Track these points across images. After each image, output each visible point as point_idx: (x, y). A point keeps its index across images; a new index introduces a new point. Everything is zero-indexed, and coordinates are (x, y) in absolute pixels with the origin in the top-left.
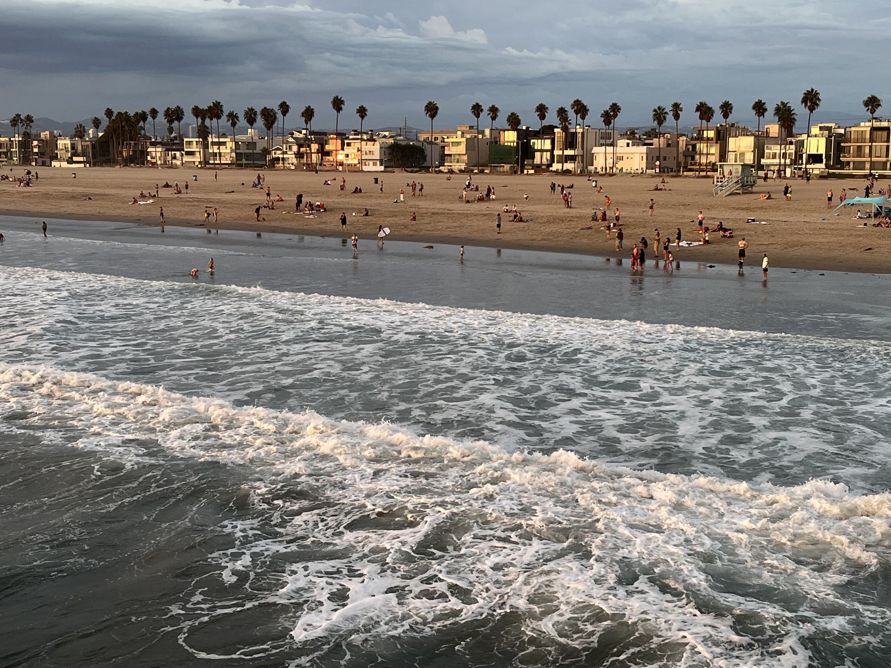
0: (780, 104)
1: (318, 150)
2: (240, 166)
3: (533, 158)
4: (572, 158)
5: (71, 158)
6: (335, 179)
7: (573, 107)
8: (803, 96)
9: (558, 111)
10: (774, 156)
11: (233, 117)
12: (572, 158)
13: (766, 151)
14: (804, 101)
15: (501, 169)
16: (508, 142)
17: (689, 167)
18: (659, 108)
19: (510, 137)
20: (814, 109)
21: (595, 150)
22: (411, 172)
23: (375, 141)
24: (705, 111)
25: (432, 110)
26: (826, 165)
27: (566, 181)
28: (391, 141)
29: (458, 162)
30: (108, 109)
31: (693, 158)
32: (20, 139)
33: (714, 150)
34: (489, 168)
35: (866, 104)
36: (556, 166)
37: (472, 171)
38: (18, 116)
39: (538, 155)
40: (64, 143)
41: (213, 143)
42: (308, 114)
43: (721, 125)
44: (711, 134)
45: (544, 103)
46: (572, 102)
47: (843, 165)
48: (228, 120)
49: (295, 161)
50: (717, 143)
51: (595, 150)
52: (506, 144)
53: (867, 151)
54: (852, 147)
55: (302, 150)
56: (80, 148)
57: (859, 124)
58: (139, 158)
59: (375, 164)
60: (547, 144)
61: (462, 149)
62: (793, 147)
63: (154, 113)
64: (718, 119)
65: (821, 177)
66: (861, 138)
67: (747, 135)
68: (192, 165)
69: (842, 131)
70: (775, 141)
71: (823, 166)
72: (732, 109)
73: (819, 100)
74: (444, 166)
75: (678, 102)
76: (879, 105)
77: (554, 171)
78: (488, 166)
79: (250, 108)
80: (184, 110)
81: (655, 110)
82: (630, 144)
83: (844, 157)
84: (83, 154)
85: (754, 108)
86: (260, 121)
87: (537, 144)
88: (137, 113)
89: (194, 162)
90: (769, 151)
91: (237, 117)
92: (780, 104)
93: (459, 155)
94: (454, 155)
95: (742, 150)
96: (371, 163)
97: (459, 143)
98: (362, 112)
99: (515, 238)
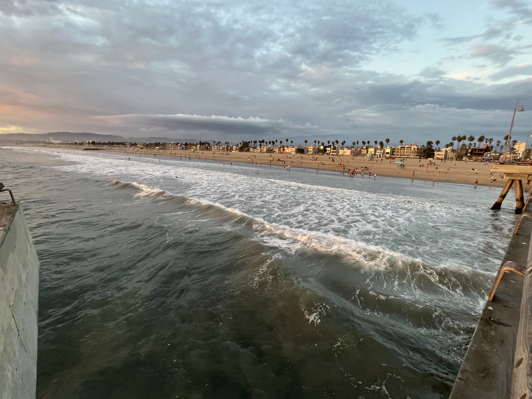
2: (267, 152)
4: (335, 152)
10: (378, 153)
14: (386, 141)
19: (322, 147)
21: (340, 150)
24: (364, 143)
25: (306, 142)
27: (333, 157)
36: (331, 154)
39: (327, 151)
40: (234, 147)
42: (281, 142)
44: (365, 148)
47: (394, 155)
51: (340, 150)
53: (399, 152)
58: (248, 150)
60: (330, 149)
63: (251, 142)
64: (367, 145)
66: (398, 149)
69: (394, 147)
71: (389, 155)
84: (238, 150)
86: (272, 143)
87: (327, 149)
98: (292, 142)
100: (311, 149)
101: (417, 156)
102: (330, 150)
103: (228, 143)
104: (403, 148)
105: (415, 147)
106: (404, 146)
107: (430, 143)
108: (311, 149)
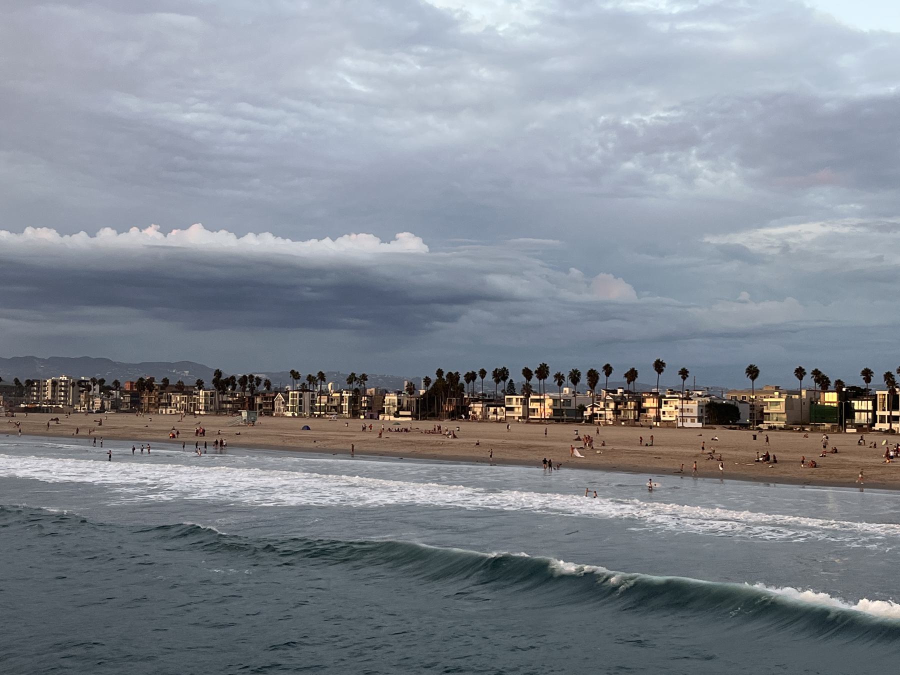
1: (635, 407)
2: (558, 421)
3: (854, 417)
5: (397, 412)
6: (701, 435)
11: (559, 378)
19: (831, 398)
22: (731, 428)
23: (690, 399)
25: (753, 372)
28: (708, 399)
29: (777, 420)
30: (439, 369)
32: (351, 395)
34: (810, 427)
36: (878, 426)
38: (353, 374)
39: (856, 414)
42: (632, 375)
48: (555, 381)
49: (612, 417)
52: (826, 404)
55: (619, 407)
56: (405, 403)
59: (693, 421)
60: (869, 405)
61: (781, 408)
63: (483, 373)
68: (512, 419)
77: (877, 431)
78: (809, 424)
80: (509, 371)
87: (857, 405)
88: (468, 373)
89: (514, 417)
91: (563, 377)
94: (772, 413)
96: (689, 420)
97: (778, 403)
98: (684, 373)
102: (874, 411)
103: (364, 377)
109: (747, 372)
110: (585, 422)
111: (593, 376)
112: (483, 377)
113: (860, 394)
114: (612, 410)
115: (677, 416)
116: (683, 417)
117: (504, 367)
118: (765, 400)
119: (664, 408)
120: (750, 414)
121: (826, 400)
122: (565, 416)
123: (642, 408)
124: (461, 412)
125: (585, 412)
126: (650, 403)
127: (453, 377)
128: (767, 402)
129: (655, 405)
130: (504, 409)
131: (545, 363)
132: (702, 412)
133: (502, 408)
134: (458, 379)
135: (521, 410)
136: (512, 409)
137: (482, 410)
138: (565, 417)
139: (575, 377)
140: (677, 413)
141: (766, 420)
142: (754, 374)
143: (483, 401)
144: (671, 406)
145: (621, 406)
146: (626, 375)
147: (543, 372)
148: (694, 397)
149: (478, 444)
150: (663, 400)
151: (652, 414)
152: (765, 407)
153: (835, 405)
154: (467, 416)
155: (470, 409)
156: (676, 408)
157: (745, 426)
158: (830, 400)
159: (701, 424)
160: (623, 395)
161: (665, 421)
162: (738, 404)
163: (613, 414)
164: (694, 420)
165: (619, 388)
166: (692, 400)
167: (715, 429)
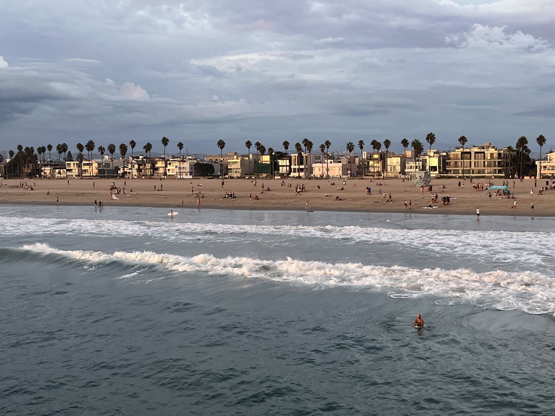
0: (414, 140)
2: (102, 177)
3: (279, 170)
4: (302, 170)
6: (191, 183)
7: (303, 142)
8: (426, 136)
9: (296, 145)
10: (411, 168)
11: (101, 149)
12: (302, 170)
13: (407, 165)
14: (427, 139)
15: (261, 176)
16: (265, 161)
17: (366, 174)
18: (350, 143)
19: (266, 159)
20: (432, 143)
21: (314, 165)
22: (209, 178)
23: (185, 161)
24: (376, 145)
25: (221, 144)
26: (439, 171)
27: (300, 182)
29: (236, 172)
31: (368, 169)
33: (380, 165)
34: (255, 176)
35: (460, 140)
36: (292, 174)
37: (244, 178)
39: (281, 168)
41: (85, 164)
42: (148, 147)
43: (382, 152)
45: (287, 141)
46: (303, 140)
47: (447, 172)
48: (99, 151)
49: (136, 173)
50: (380, 161)
51: (314, 165)
52: (263, 162)
53: (460, 164)
54: (452, 163)
55: (141, 167)
57: (455, 150)
59: (186, 175)
60: (286, 162)
61: (238, 165)
62: (421, 163)
63: (50, 147)
64: (383, 149)
65: (437, 178)
67: (395, 157)
69: (445, 154)
70: (410, 159)
71: (437, 172)
72: (390, 143)
73: (435, 138)
74: (228, 175)
75: (362, 140)
76: (466, 141)
77: (292, 177)
79: (111, 144)
80: (68, 145)
81: (348, 144)
82: (332, 162)
83: (448, 167)
85: (402, 142)
89: (72, 175)
90: (408, 165)
91: (104, 149)
92: (414, 140)
93: (236, 168)
95: (394, 164)
96: (184, 174)
97: (236, 162)
98: (180, 146)
99: (345, 207)
100: (235, 164)
101: (500, 171)
104: (466, 155)
105: (492, 150)
106: (468, 150)
107: (523, 141)
108: (235, 164)
109: (218, 144)
110: (119, 177)
111: (123, 148)
112: (50, 150)
113: (282, 156)
114: (136, 169)
115: (177, 172)
116: (180, 172)
117: (64, 143)
118: (229, 161)
119: (169, 167)
120: (220, 170)
121: (264, 160)
122: (106, 173)
123: (155, 167)
124: (36, 173)
125: (119, 171)
126: (160, 164)
127: (30, 151)
128: (230, 162)
129: (163, 165)
130: (65, 170)
131: (92, 140)
132: (192, 169)
133: (64, 170)
134: (33, 151)
135: (77, 171)
136: (70, 170)
137: (50, 171)
138: (106, 174)
139: (112, 149)
140: (177, 170)
141: (230, 173)
142: (222, 145)
143: (51, 165)
144: (173, 166)
145: (142, 167)
146: (144, 147)
147: (90, 146)
148: (187, 160)
149: (48, 194)
150: (168, 162)
151: (161, 171)
152: (229, 165)
153: (269, 163)
154: (40, 176)
155: (42, 171)
156: (176, 167)
157: (218, 177)
158: (266, 160)
159: (191, 176)
160: (143, 160)
161: (169, 175)
162: (213, 164)
163: (137, 172)
164: (187, 174)
165: (140, 155)
166: (186, 162)
167: (200, 179)
